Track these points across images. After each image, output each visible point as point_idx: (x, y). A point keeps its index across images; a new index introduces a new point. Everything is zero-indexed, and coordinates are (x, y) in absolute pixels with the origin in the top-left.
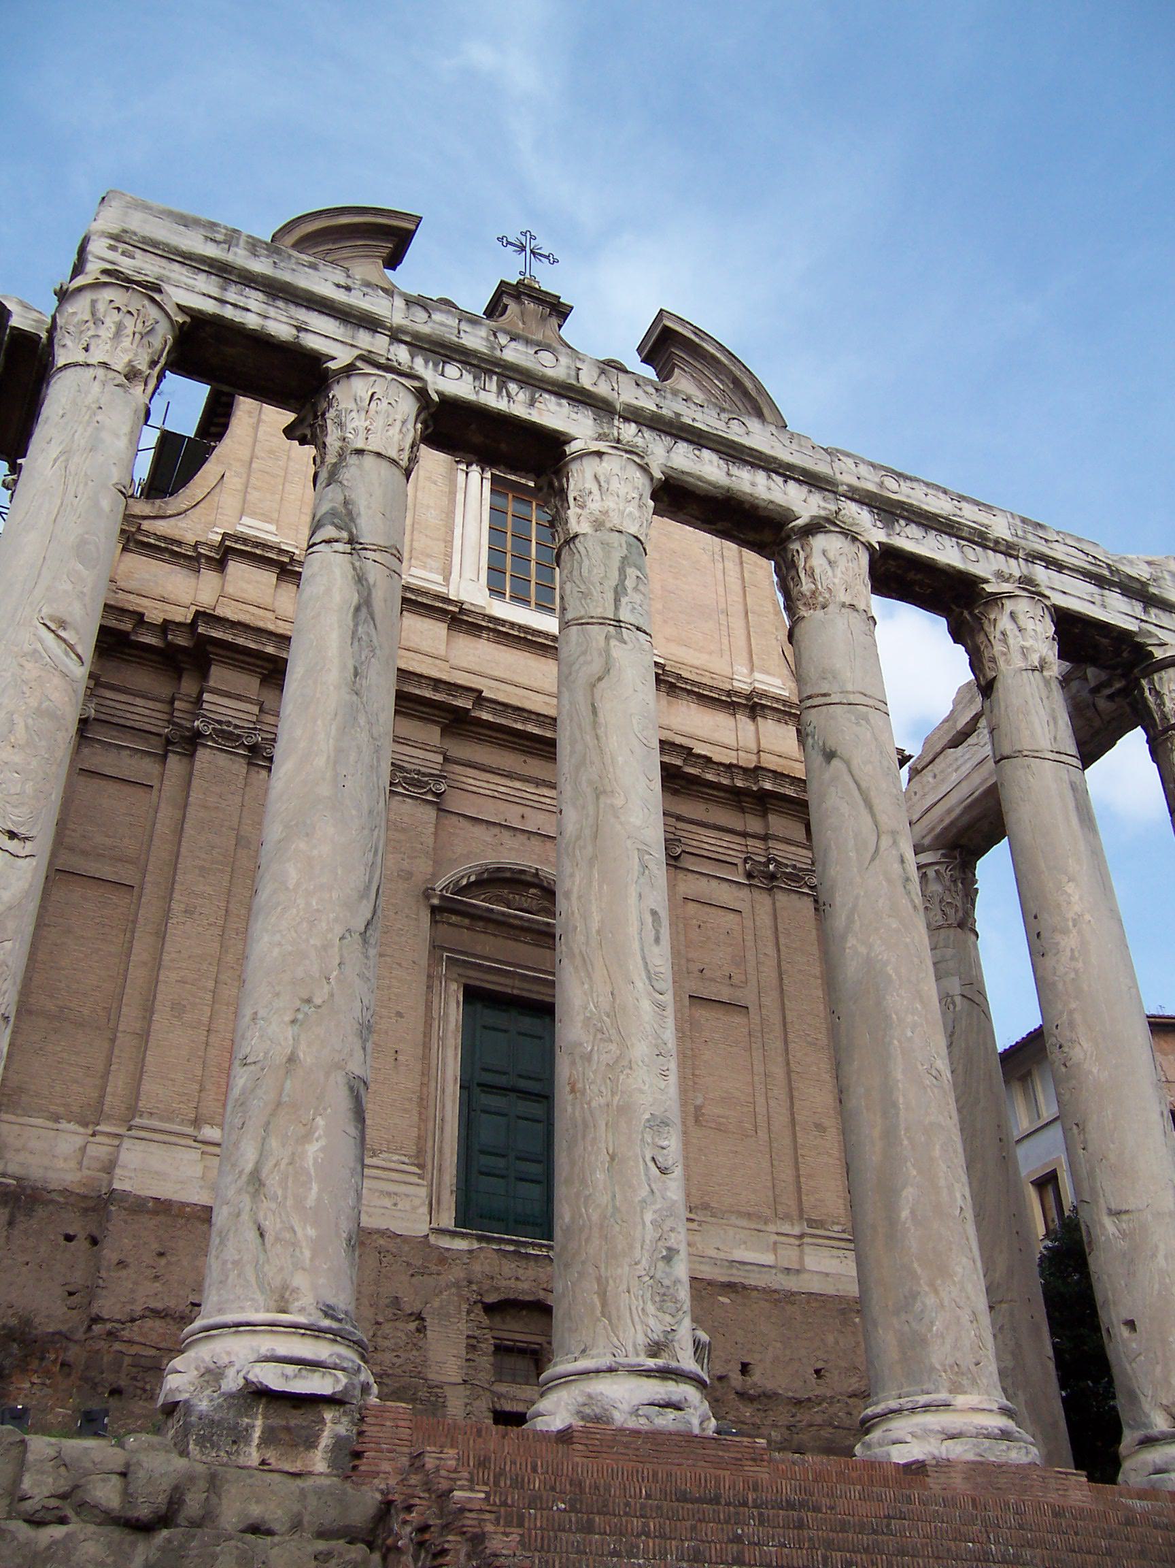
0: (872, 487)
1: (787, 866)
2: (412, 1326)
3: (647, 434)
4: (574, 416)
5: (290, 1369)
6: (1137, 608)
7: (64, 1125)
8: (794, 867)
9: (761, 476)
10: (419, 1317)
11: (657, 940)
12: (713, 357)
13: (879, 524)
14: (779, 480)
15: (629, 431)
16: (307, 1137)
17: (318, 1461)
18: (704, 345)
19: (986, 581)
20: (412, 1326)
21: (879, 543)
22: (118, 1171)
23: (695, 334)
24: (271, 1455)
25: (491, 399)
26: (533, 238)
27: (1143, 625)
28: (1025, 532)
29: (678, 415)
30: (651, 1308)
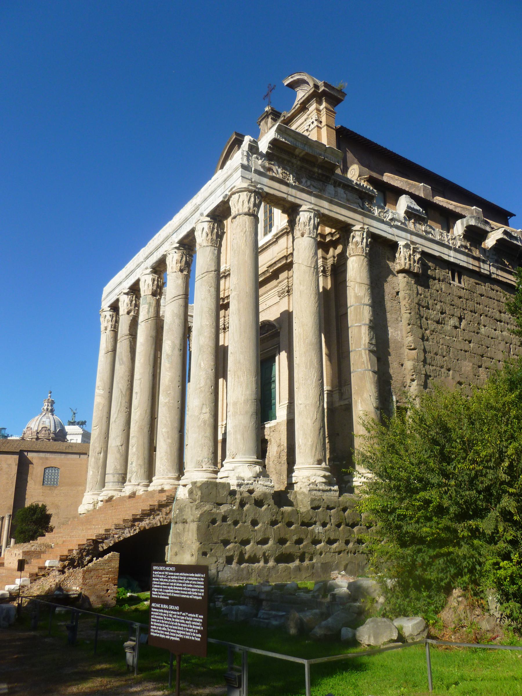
21: (177, 243)
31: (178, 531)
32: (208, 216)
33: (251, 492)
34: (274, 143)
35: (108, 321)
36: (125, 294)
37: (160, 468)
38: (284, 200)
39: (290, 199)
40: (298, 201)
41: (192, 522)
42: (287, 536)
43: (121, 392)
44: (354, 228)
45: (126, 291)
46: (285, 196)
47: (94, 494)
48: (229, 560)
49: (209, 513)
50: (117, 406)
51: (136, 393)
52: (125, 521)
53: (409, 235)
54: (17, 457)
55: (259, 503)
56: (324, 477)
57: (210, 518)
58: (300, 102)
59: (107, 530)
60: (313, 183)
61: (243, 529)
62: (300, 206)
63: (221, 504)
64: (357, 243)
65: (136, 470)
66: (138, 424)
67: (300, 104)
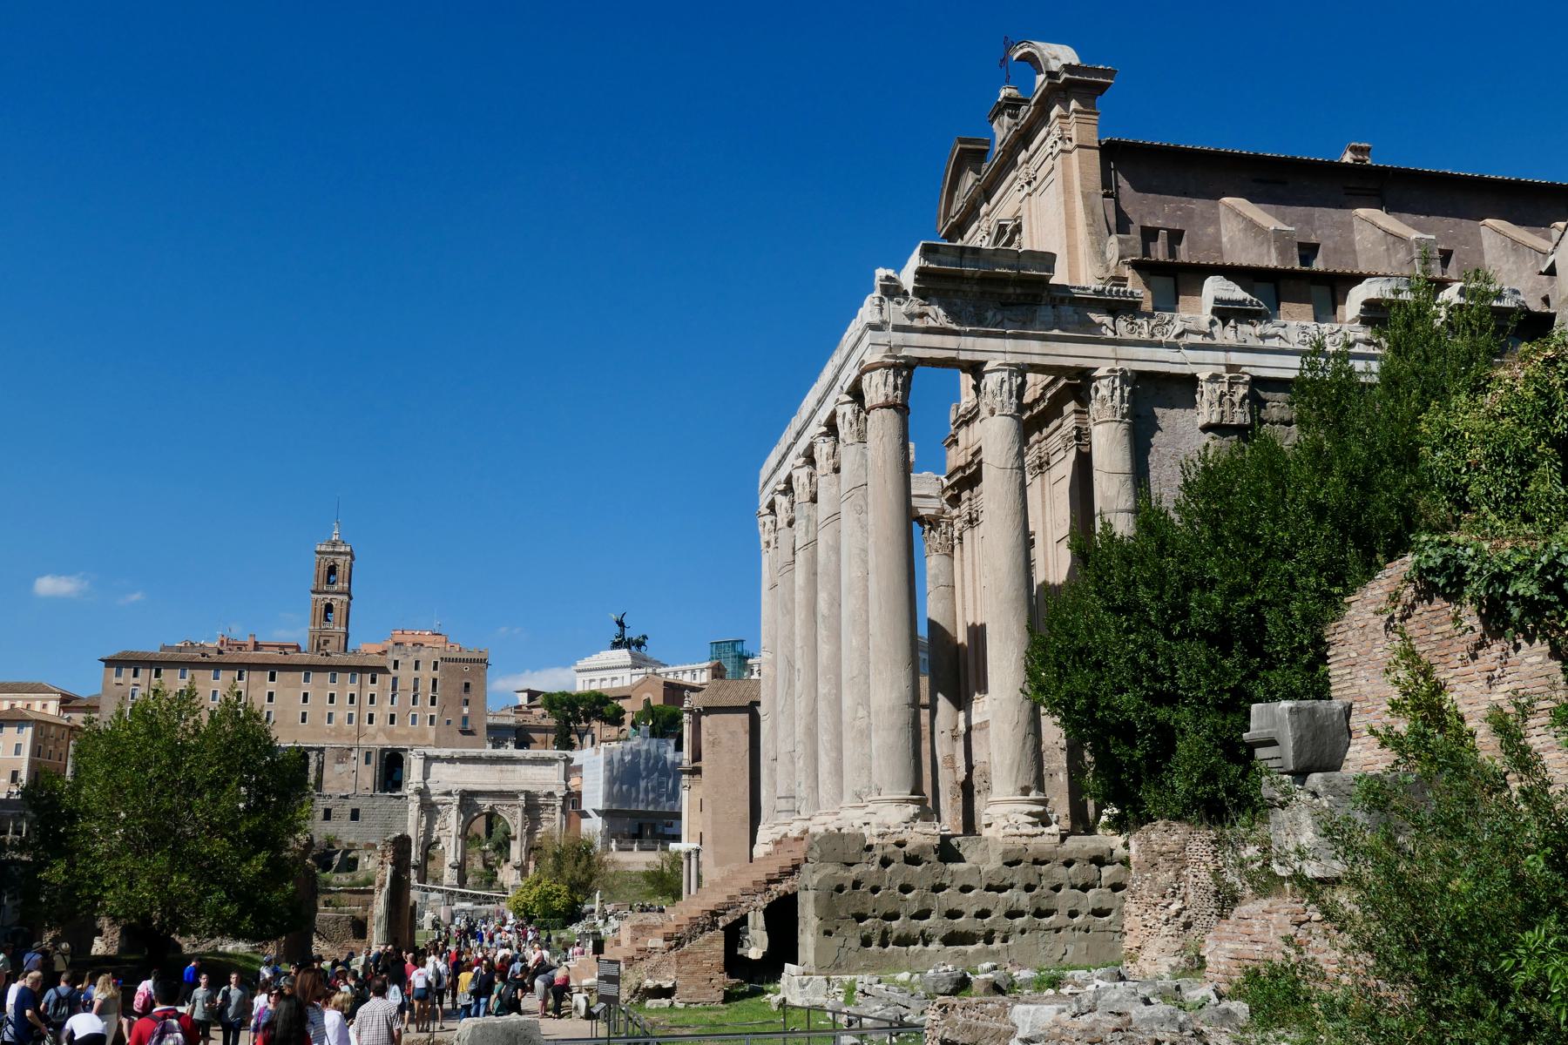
33: (901, 844)
34: (921, 274)
38: (953, 359)
39: (964, 356)
40: (979, 357)
42: (963, 908)
44: (1096, 374)
46: (953, 354)
48: (866, 942)
49: (832, 876)
52: (754, 883)
53: (1221, 354)
54: (746, 716)
55: (912, 860)
56: (1030, 814)
57: (834, 884)
59: (730, 897)
60: (1007, 313)
61: (885, 900)
62: (984, 363)
63: (852, 864)
64: (1103, 399)
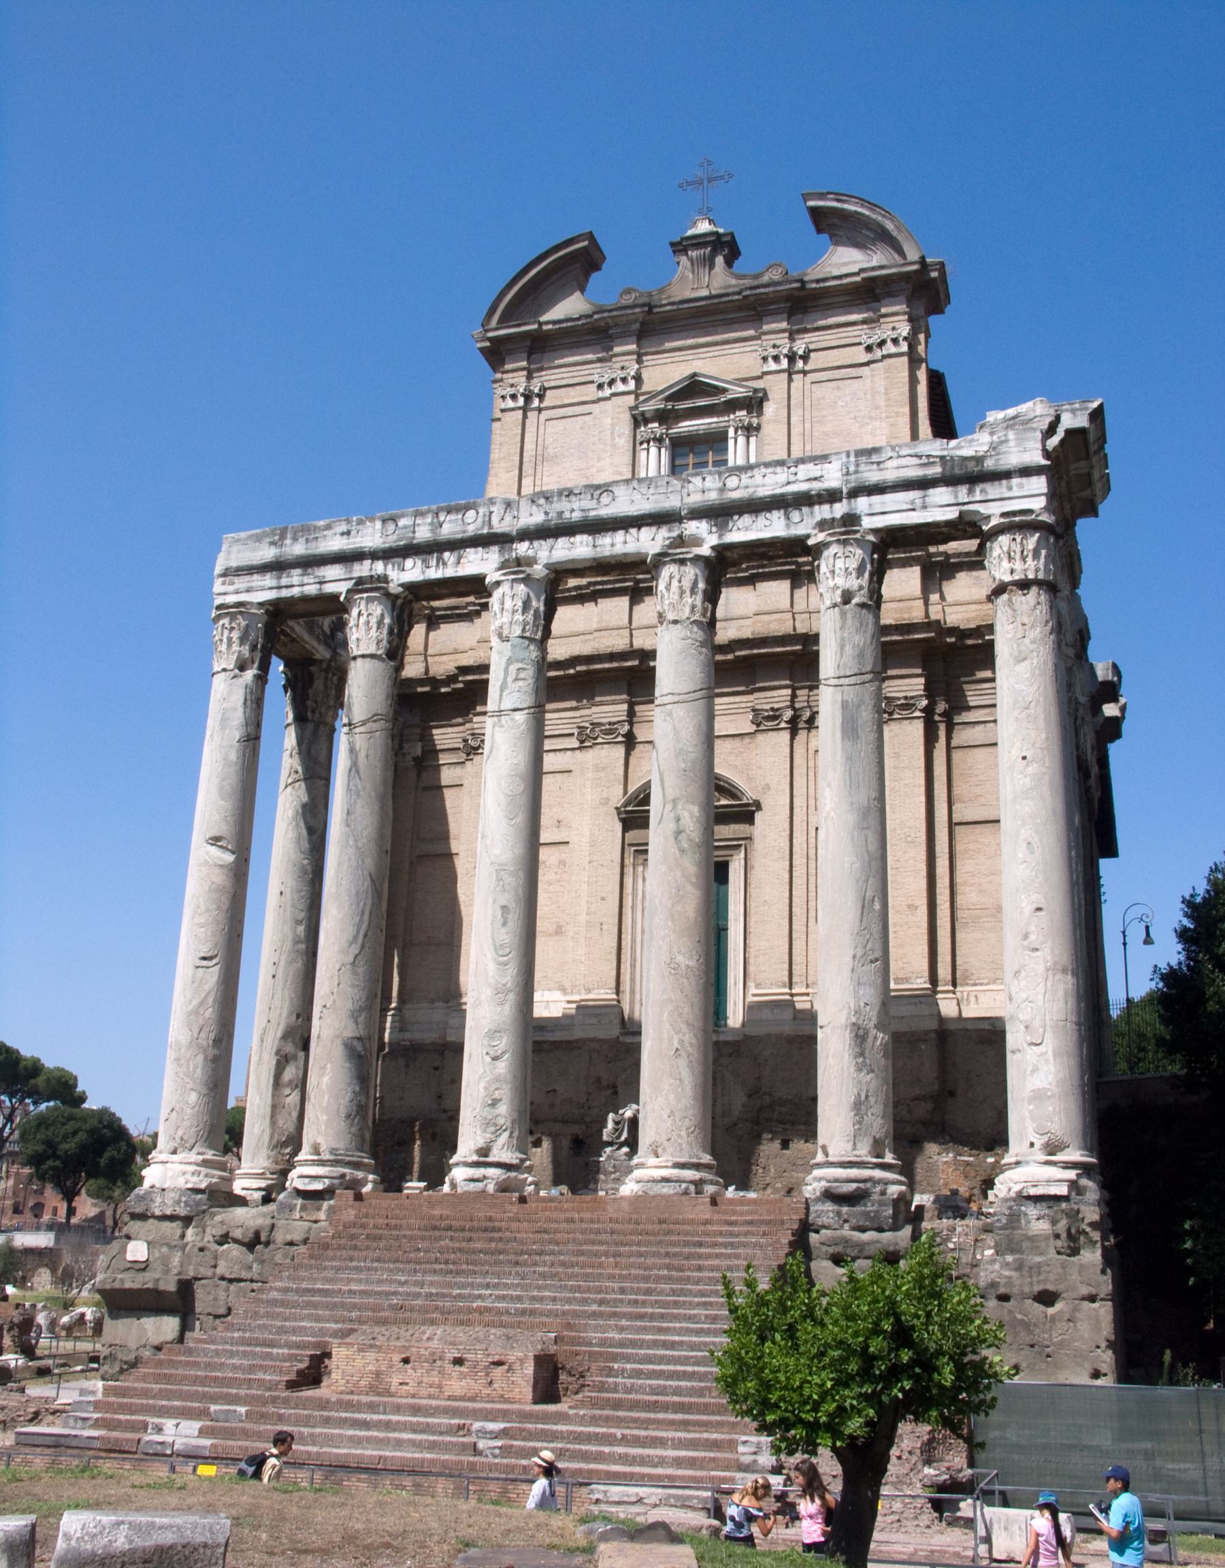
0: (713, 496)
1: (899, 699)
2: (609, 1092)
3: (536, 543)
4: (486, 556)
5: (307, 1180)
6: (963, 491)
7: (437, 1004)
8: (906, 698)
9: (620, 536)
10: (615, 1087)
11: (504, 924)
12: (859, 213)
13: (714, 529)
14: (633, 531)
15: (522, 548)
16: (323, 1074)
17: (322, 1215)
18: (846, 206)
19: (808, 536)
20: (609, 1092)
21: (713, 548)
22: (448, 1031)
23: (838, 200)
24: (304, 1214)
25: (434, 573)
26: (709, 163)
27: (966, 508)
28: (857, 465)
29: (561, 513)
30: (479, 1132)
31: (1019, 1316)
32: (875, 531)
35: (253, 648)
36: (387, 595)
37: (680, 1136)
41: (1083, 1299)
43: (372, 880)
45: (394, 588)
47: (205, 1163)
50: (361, 921)
51: (504, 908)
58: (864, 275)
65: (509, 1124)
66: (512, 997)
67: (864, 279)
